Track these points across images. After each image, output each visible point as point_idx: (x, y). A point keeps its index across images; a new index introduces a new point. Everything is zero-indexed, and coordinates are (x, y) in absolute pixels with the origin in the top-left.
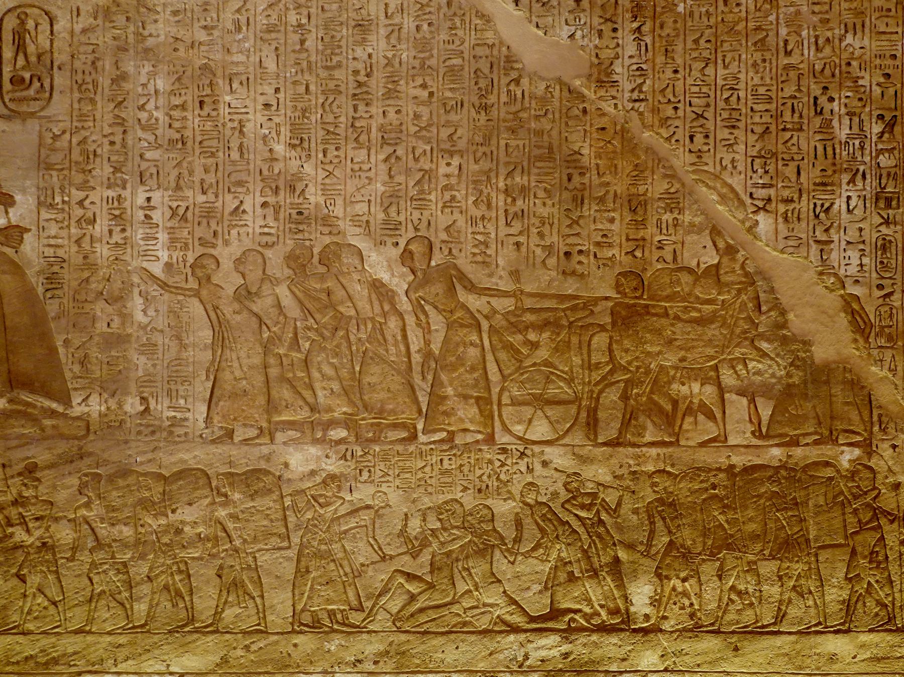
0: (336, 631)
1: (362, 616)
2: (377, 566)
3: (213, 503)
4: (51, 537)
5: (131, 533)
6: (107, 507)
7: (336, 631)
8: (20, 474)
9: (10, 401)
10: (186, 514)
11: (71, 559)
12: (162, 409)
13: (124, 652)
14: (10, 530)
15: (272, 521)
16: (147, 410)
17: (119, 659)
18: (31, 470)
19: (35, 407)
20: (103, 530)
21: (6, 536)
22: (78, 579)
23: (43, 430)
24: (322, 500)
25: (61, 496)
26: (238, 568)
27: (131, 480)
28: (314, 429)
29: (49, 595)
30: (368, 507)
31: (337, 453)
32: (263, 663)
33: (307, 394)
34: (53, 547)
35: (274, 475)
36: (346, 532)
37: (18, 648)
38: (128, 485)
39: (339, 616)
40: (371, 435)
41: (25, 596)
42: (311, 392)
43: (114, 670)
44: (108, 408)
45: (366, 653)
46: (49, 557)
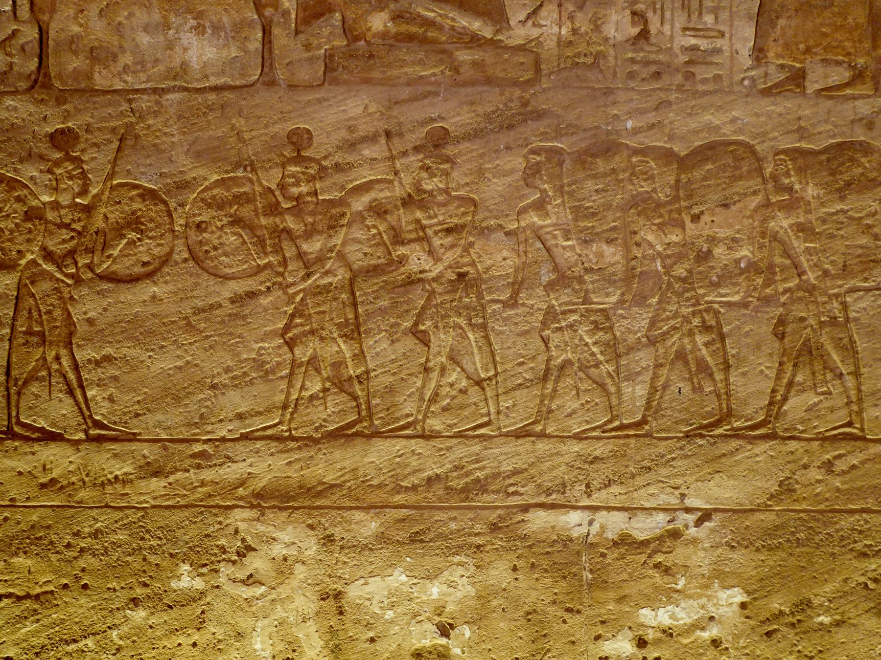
3: (767, 204)
4: (473, 264)
5: (618, 257)
6: (575, 210)
8: (417, 149)
9: (397, 17)
10: (718, 225)
11: (512, 303)
12: (673, 33)
13: (605, 470)
14: (402, 250)
16: (644, 34)
17: (595, 484)
18: (437, 142)
19: (440, 28)
20: (568, 250)
21: (391, 262)
22: (522, 339)
23: (456, 70)
25: (493, 189)
26: (812, 321)
27: (618, 161)
37: (414, 463)
41: (427, 370)
43: (586, 502)
44: (574, 31)
46: (470, 299)
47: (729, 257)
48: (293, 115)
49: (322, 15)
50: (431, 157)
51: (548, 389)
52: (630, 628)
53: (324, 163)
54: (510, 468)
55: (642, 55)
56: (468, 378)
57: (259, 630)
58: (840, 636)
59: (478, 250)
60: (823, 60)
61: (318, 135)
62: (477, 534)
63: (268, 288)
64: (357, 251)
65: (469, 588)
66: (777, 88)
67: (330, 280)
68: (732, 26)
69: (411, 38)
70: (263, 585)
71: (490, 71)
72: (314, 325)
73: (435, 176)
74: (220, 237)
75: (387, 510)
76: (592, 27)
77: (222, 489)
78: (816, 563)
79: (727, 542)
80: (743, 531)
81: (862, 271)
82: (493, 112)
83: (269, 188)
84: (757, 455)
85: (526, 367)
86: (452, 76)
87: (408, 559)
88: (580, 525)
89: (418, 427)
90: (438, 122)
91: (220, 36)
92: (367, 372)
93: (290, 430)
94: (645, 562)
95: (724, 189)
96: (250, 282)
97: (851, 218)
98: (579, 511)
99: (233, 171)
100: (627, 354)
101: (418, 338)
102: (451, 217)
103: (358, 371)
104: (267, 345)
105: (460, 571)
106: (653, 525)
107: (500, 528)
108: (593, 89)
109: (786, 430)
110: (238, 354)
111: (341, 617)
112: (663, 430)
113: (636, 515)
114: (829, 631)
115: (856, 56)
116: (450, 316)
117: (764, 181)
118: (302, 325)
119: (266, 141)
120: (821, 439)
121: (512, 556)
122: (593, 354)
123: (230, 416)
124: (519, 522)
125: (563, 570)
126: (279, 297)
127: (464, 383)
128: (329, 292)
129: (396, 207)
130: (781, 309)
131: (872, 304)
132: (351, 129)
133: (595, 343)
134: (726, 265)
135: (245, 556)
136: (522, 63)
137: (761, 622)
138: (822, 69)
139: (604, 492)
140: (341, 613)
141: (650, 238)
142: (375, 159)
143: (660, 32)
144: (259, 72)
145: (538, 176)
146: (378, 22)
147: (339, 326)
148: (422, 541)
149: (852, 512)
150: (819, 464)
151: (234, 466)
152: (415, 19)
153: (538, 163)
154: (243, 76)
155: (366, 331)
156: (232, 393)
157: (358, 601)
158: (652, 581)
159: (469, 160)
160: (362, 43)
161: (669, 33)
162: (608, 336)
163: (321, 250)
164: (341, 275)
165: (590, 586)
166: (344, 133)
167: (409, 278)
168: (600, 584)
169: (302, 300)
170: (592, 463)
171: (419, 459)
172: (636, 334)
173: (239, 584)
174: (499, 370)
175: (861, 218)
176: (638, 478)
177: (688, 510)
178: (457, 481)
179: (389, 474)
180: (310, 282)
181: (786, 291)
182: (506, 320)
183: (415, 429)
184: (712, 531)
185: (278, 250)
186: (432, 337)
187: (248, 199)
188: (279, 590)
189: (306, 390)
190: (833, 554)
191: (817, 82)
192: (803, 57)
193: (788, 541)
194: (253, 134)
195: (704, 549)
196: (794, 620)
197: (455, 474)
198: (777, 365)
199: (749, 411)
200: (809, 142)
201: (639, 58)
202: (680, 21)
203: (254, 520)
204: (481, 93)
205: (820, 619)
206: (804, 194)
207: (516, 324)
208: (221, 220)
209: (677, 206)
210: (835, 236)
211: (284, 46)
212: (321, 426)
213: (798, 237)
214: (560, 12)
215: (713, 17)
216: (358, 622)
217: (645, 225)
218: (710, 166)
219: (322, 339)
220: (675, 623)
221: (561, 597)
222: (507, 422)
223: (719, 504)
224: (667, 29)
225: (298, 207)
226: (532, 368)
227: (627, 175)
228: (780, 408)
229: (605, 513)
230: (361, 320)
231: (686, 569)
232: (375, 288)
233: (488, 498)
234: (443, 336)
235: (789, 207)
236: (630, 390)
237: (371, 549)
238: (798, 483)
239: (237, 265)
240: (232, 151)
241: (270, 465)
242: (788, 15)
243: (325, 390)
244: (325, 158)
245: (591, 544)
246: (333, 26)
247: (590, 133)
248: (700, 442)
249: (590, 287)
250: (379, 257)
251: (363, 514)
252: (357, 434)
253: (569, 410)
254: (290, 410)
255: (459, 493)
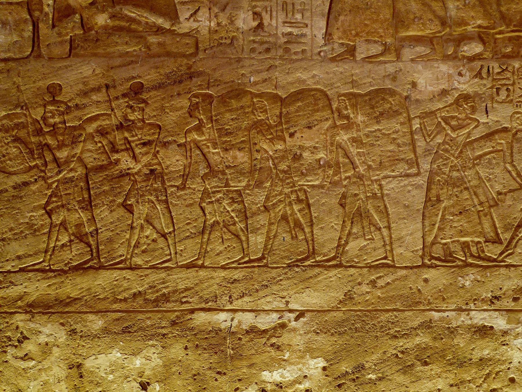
0: (471, 265)
1: (499, 249)
2: (515, 194)
3: (334, 126)
4: (159, 164)
5: (246, 159)
6: (219, 130)
7: (471, 265)
8: (124, 95)
9: (113, 17)
11: (183, 187)
12: (277, 25)
13: (240, 287)
14: (116, 156)
15: (399, 146)
16: (260, 26)
17: (235, 296)
18: (137, 91)
19: (139, 23)
20: (215, 154)
22: (189, 209)
23: (148, 48)
24: (454, 123)
25: (170, 119)
26: (362, 196)
27: (245, 101)
28: (445, 43)
29: (158, 227)
30: (505, 130)
31: (471, 70)
32: (392, 299)
33: (436, 6)
34: (162, 175)
35: (400, 94)
36: (480, 157)
37: (125, 284)
38: (242, 107)
39: (474, 249)
40: (509, 50)
41: (132, 228)
42: (441, 4)
44: (219, 24)
45: (504, 289)
46: (158, 185)
47: (312, 158)
48: (50, 75)
49: (69, 16)
50: (133, 100)
51: (205, 238)
52: (256, 383)
53: (69, 104)
54: (183, 287)
55: (259, 38)
56: (158, 232)
57: (32, 388)
58: (381, 386)
59: (162, 156)
60: (366, 40)
61: (65, 88)
62: (163, 328)
63: (36, 180)
64: (90, 157)
65: (158, 360)
66: (339, 57)
67: (73, 175)
68: (312, 20)
69: (120, 29)
70: (34, 360)
71: (169, 48)
72: (64, 202)
73: (136, 111)
74: (7, 149)
75: (109, 314)
76: (229, 21)
77: (8, 302)
78: (367, 342)
79: (314, 330)
80: (324, 323)
81: (391, 166)
82: (170, 73)
83: (36, 119)
84: (331, 277)
85: (191, 226)
86: (146, 52)
87: (121, 343)
88: (226, 321)
89: (127, 263)
90: (137, 79)
91: (6, 29)
92: (97, 230)
93: (50, 265)
94: (265, 343)
95: (308, 117)
96: (25, 176)
97: (384, 134)
98: (225, 313)
99: (14, 109)
100: (252, 217)
101: (127, 209)
102: (145, 136)
103: (91, 229)
104: (35, 214)
105: (153, 350)
106: (270, 320)
107: (177, 323)
108: (230, 58)
109: (347, 262)
110: (17, 220)
111: (81, 379)
112: (275, 263)
113: (259, 314)
114: (375, 384)
115: (385, 38)
116: (145, 195)
117: (333, 113)
118: (56, 202)
119: (33, 91)
120: (369, 267)
121: (184, 340)
122: (232, 217)
123: (13, 257)
124: (189, 320)
125: (215, 348)
126: (42, 185)
127: (155, 236)
128: (73, 181)
129: (113, 130)
130: (344, 189)
131: (397, 185)
132: (85, 84)
133: (233, 211)
134: (311, 163)
135: (22, 343)
136: (188, 44)
137: (335, 378)
138: (366, 46)
139: (240, 301)
140: (81, 377)
141: (265, 147)
142: (100, 102)
143: (270, 24)
144: (30, 50)
145: (197, 110)
146: (102, 19)
147: (79, 202)
148: (129, 332)
149: (388, 311)
150: (368, 282)
151: (15, 288)
152: (123, 18)
153: (197, 103)
154: (20, 52)
155: (95, 205)
156: (14, 243)
157: (92, 369)
158: (269, 354)
159: (155, 102)
160: (93, 32)
161: (275, 25)
162: (240, 206)
163: (68, 156)
164: (80, 171)
165: (232, 358)
166: (81, 86)
167: (121, 173)
168: (238, 356)
169: (57, 186)
170: (232, 283)
171: (128, 282)
172: (257, 204)
173: (19, 360)
174: (176, 228)
175: (390, 134)
176: (260, 292)
177: (291, 311)
178: (151, 295)
179: (110, 292)
180: (61, 176)
181: (346, 178)
182: (178, 197)
183: (126, 263)
184: (305, 323)
185: (42, 156)
186: (135, 208)
187: (24, 126)
188: (43, 363)
189: (59, 241)
190: (377, 336)
191: (362, 53)
192: (354, 39)
193: (350, 329)
194: (27, 87)
195: (300, 335)
196: (354, 377)
197: (150, 291)
198: (342, 222)
199: (325, 251)
200: (358, 89)
201: (257, 40)
202: (282, 17)
203: (28, 320)
204: (162, 61)
205: (370, 376)
206: (356, 120)
207: (185, 200)
208: (7, 139)
209: (281, 128)
210: (375, 145)
211: (46, 34)
212: (69, 263)
213: (353, 146)
214: (210, 13)
215: (301, 15)
216: (92, 382)
217: (262, 139)
218: (300, 104)
219: (69, 210)
220: (284, 380)
221: (214, 365)
222: (181, 259)
223: (309, 307)
224: (274, 22)
225: (54, 130)
226: (195, 226)
227: (250, 109)
228: (344, 248)
229: (241, 313)
230: (92, 198)
231: (289, 346)
232: (101, 179)
233: (169, 306)
234: (141, 208)
235: (347, 128)
236: (254, 239)
237: (99, 337)
238: (355, 293)
239: (17, 166)
240: (14, 97)
241: (37, 287)
242: (345, 14)
243: (71, 241)
244: (70, 101)
245: (233, 332)
246: (75, 22)
247: (228, 85)
248: (297, 269)
249: (229, 177)
250: (103, 161)
251: (94, 316)
252: (91, 267)
253: (218, 252)
254: (50, 253)
255: (152, 303)
